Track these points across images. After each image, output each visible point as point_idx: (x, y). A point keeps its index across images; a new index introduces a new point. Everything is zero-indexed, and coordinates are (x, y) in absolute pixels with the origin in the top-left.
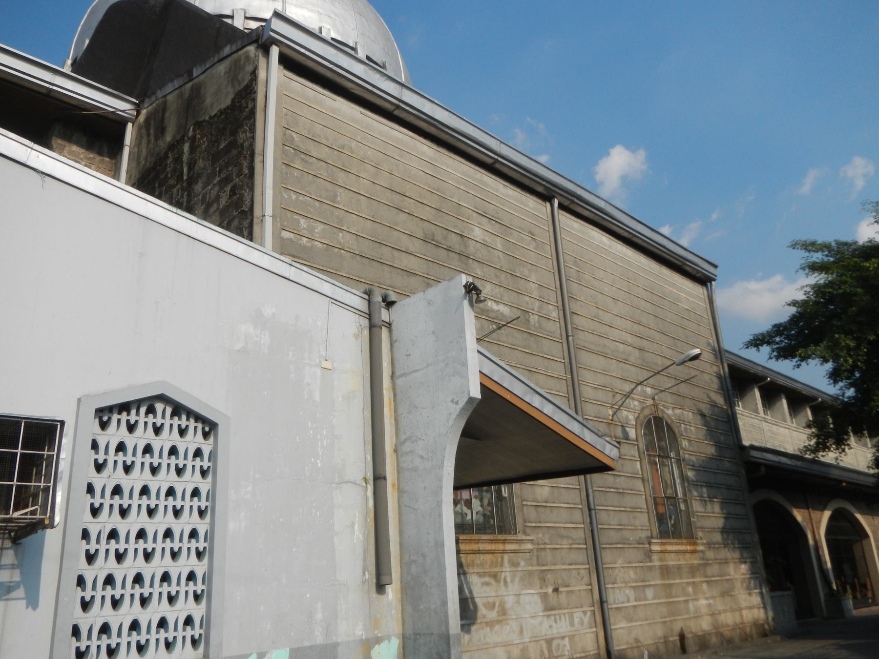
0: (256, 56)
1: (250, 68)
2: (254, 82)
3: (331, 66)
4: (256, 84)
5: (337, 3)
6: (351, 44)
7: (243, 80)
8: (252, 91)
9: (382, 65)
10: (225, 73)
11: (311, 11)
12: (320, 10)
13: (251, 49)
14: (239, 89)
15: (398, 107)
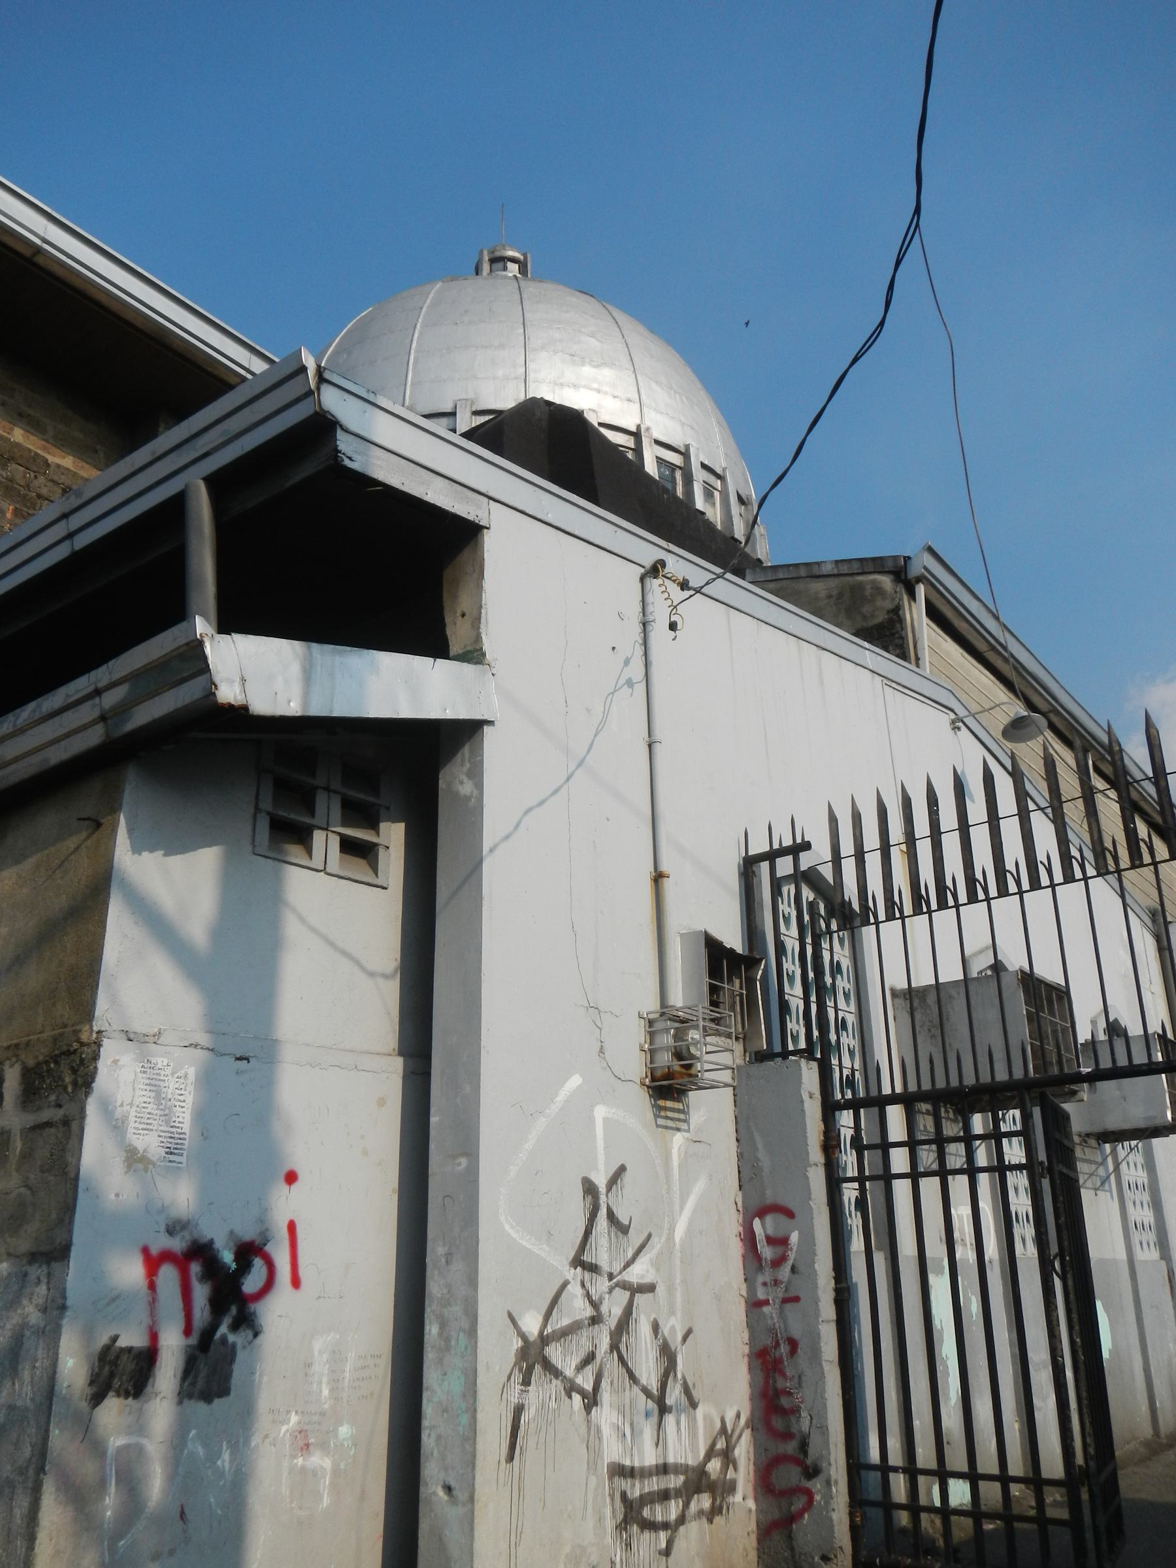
0: (896, 592)
1: (888, 605)
2: (898, 625)
3: (957, 605)
4: (902, 629)
5: (696, 407)
6: (719, 471)
7: (873, 616)
8: (893, 635)
9: (745, 500)
10: (830, 596)
11: (673, 418)
12: (683, 419)
13: (886, 581)
14: (864, 624)
15: (993, 648)
